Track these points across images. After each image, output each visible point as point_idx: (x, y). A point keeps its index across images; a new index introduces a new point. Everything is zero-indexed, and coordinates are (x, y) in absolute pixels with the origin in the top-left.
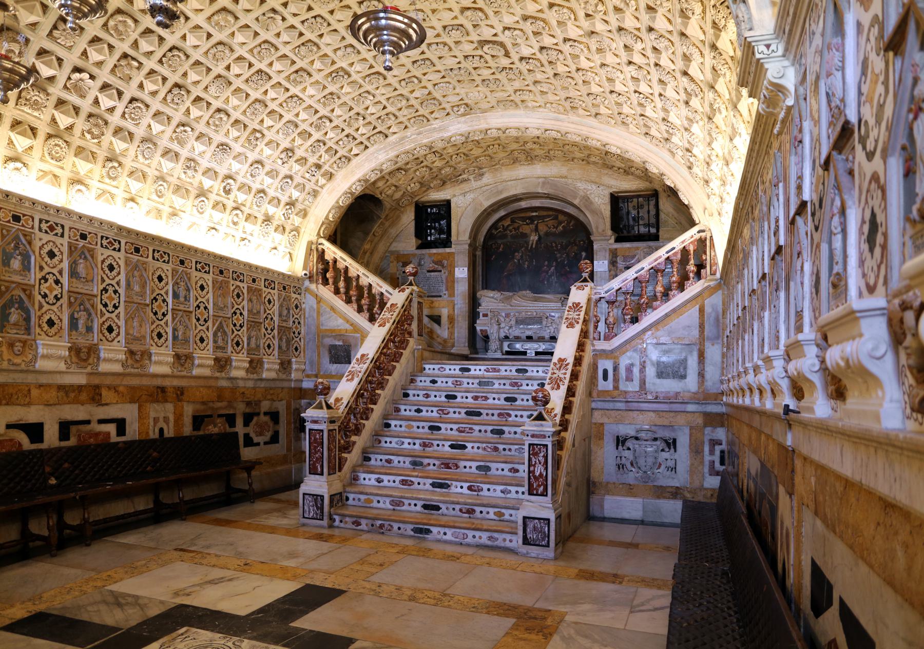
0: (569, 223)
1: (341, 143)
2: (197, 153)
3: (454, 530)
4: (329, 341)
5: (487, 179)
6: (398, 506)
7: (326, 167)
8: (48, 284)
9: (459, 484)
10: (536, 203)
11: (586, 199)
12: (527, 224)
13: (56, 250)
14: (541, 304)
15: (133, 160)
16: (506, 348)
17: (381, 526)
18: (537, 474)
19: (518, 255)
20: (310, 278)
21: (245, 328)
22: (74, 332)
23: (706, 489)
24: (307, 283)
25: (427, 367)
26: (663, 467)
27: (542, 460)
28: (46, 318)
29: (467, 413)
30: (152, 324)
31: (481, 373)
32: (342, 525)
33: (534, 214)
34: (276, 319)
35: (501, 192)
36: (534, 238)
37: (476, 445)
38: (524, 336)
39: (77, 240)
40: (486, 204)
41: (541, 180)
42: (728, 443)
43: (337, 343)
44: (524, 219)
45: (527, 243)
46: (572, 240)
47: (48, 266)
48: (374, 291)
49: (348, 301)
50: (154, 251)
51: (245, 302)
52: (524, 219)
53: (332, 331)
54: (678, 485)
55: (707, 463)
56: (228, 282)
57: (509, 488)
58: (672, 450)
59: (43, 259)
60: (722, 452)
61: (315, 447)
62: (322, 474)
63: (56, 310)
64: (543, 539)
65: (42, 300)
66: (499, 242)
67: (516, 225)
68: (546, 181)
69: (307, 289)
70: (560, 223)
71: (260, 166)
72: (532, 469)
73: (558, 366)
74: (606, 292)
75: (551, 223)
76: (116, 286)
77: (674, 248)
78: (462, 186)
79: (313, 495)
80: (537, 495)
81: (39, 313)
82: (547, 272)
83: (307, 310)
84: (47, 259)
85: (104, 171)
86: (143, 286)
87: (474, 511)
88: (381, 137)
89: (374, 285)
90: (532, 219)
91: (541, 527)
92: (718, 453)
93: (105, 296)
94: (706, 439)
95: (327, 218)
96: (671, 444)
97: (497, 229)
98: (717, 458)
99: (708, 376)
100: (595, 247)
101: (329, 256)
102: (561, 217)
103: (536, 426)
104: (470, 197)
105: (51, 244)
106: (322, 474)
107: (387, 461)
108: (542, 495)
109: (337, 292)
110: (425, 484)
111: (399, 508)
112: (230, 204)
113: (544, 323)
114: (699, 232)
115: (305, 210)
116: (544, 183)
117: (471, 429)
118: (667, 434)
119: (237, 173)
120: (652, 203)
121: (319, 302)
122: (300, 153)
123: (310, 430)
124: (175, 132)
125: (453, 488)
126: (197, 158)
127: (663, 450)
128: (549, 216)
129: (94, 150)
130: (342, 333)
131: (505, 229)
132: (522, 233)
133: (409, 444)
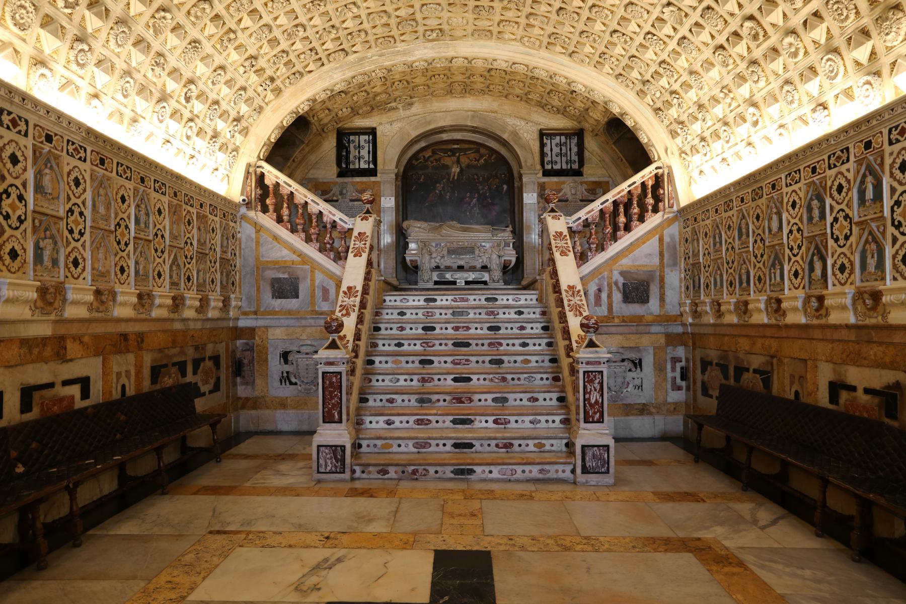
0: (490, 157)
1: (302, 56)
2: (168, 47)
3: (501, 467)
4: (271, 274)
5: (417, 109)
6: (424, 447)
7: (278, 82)
9: (483, 418)
10: (458, 136)
11: (515, 134)
14: (471, 234)
15: (103, 46)
16: (435, 278)
17: (414, 472)
18: (593, 401)
19: (439, 186)
20: (248, 204)
21: (194, 261)
22: (39, 267)
23: (669, 403)
24: (243, 210)
25: (387, 298)
26: (631, 386)
27: (598, 387)
29: (454, 345)
30: (116, 255)
31: (448, 303)
32: (364, 476)
33: (456, 146)
34: (218, 249)
35: (429, 123)
36: (455, 170)
37: (482, 377)
38: (455, 266)
40: (414, 134)
41: (469, 113)
42: (687, 360)
43: (281, 276)
45: (449, 175)
46: (494, 173)
47: (11, 175)
48: (325, 219)
49: (293, 231)
51: (195, 231)
52: (445, 151)
53: (275, 262)
54: (644, 402)
55: (669, 380)
56: (181, 206)
57: (538, 417)
58: (639, 369)
59: (4, 165)
60: (682, 368)
61: (331, 392)
62: (340, 421)
63: (19, 236)
64: (603, 466)
66: (420, 172)
67: (437, 157)
68: (475, 114)
69: (244, 217)
70: (482, 156)
71: (223, 73)
72: (587, 396)
73: (570, 293)
74: (574, 222)
75: (472, 156)
76: (81, 205)
77: (635, 183)
78: (390, 114)
79: (331, 446)
80: (593, 422)
82: (470, 204)
83: (243, 240)
85: (72, 54)
86: (108, 208)
87: (512, 445)
88: (342, 54)
89: (325, 212)
90: (453, 151)
91: (601, 454)
92: (678, 370)
94: (669, 357)
95: (269, 139)
96: (638, 364)
97: (417, 160)
98: (678, 374)
99: (668, 299)
100: (524, 180)
101: (269, 181)
102: (482, 151)
103: (591, 353)
104: (396, 126)
105: (14, 144)
106: (340, 421)
107: (388, 401)
108: (598, 422)
109: (279, 220)
110: (444, 422)
111: (424, 450)
112: (187, 115)
113: (477, 252)
114: (657, 168)
115: (247, 128)
116: (473, 117)
117: (467, 360)
118: (633, 355)
119: (199, 78)
120: (575, 141)
121: (258, 231)
122: (261, 63)
123: (323, 373)
124: (153, 17)
125: (476, 423)
126: (167, 53)
127: (630, 370)
128: (470, 149)
129: (64, 24)
130: (288, 264)
132: (443, 165)
133: (406, 380)
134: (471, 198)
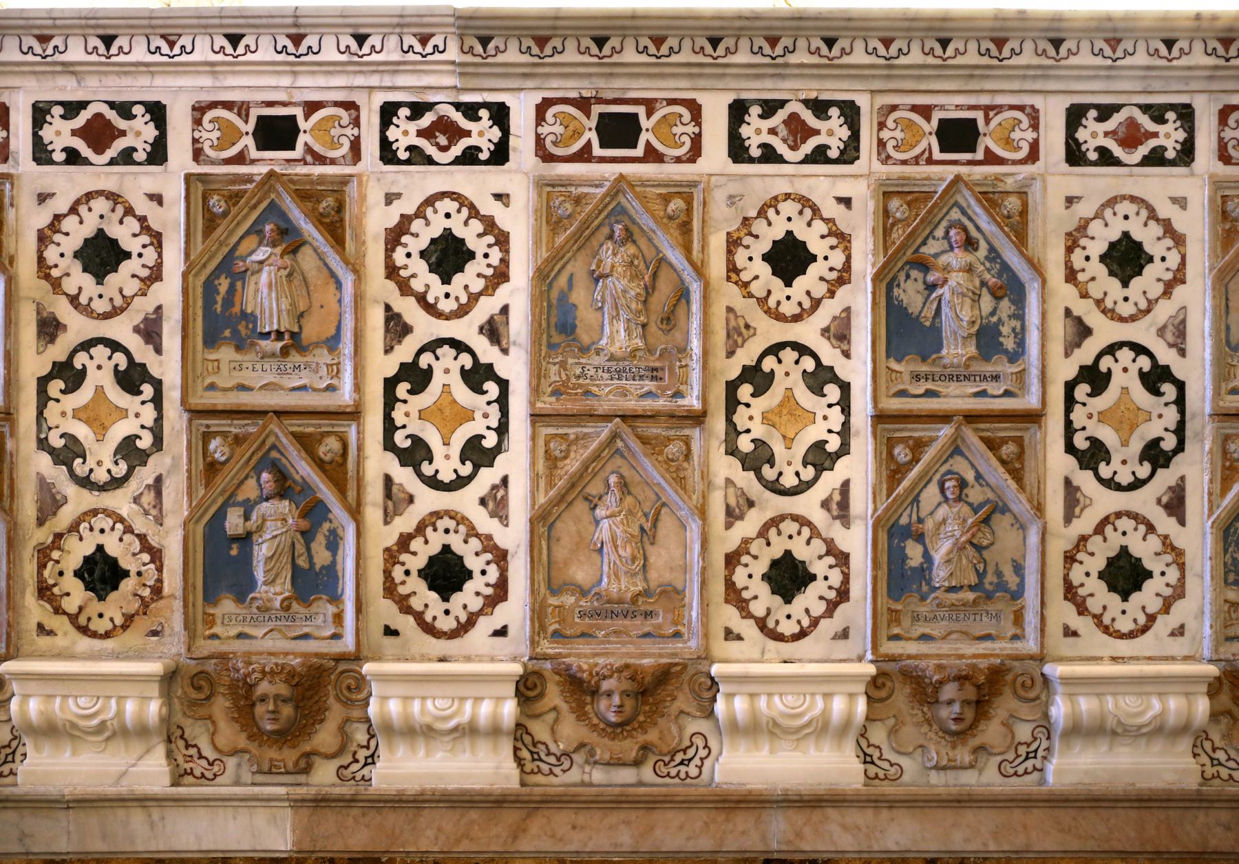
8: (84, 394)
13: (125, 234)
22: (228, 605)
28: (78, 551)
30: (733, 516)
39: (240, 159)
47: (87, 311)
50: (738, 111)
59: (56, 285)
65: (57, 475)
81: (43, 536)
84: (79, 280)
93: (410, 412)
105: (100, 205)
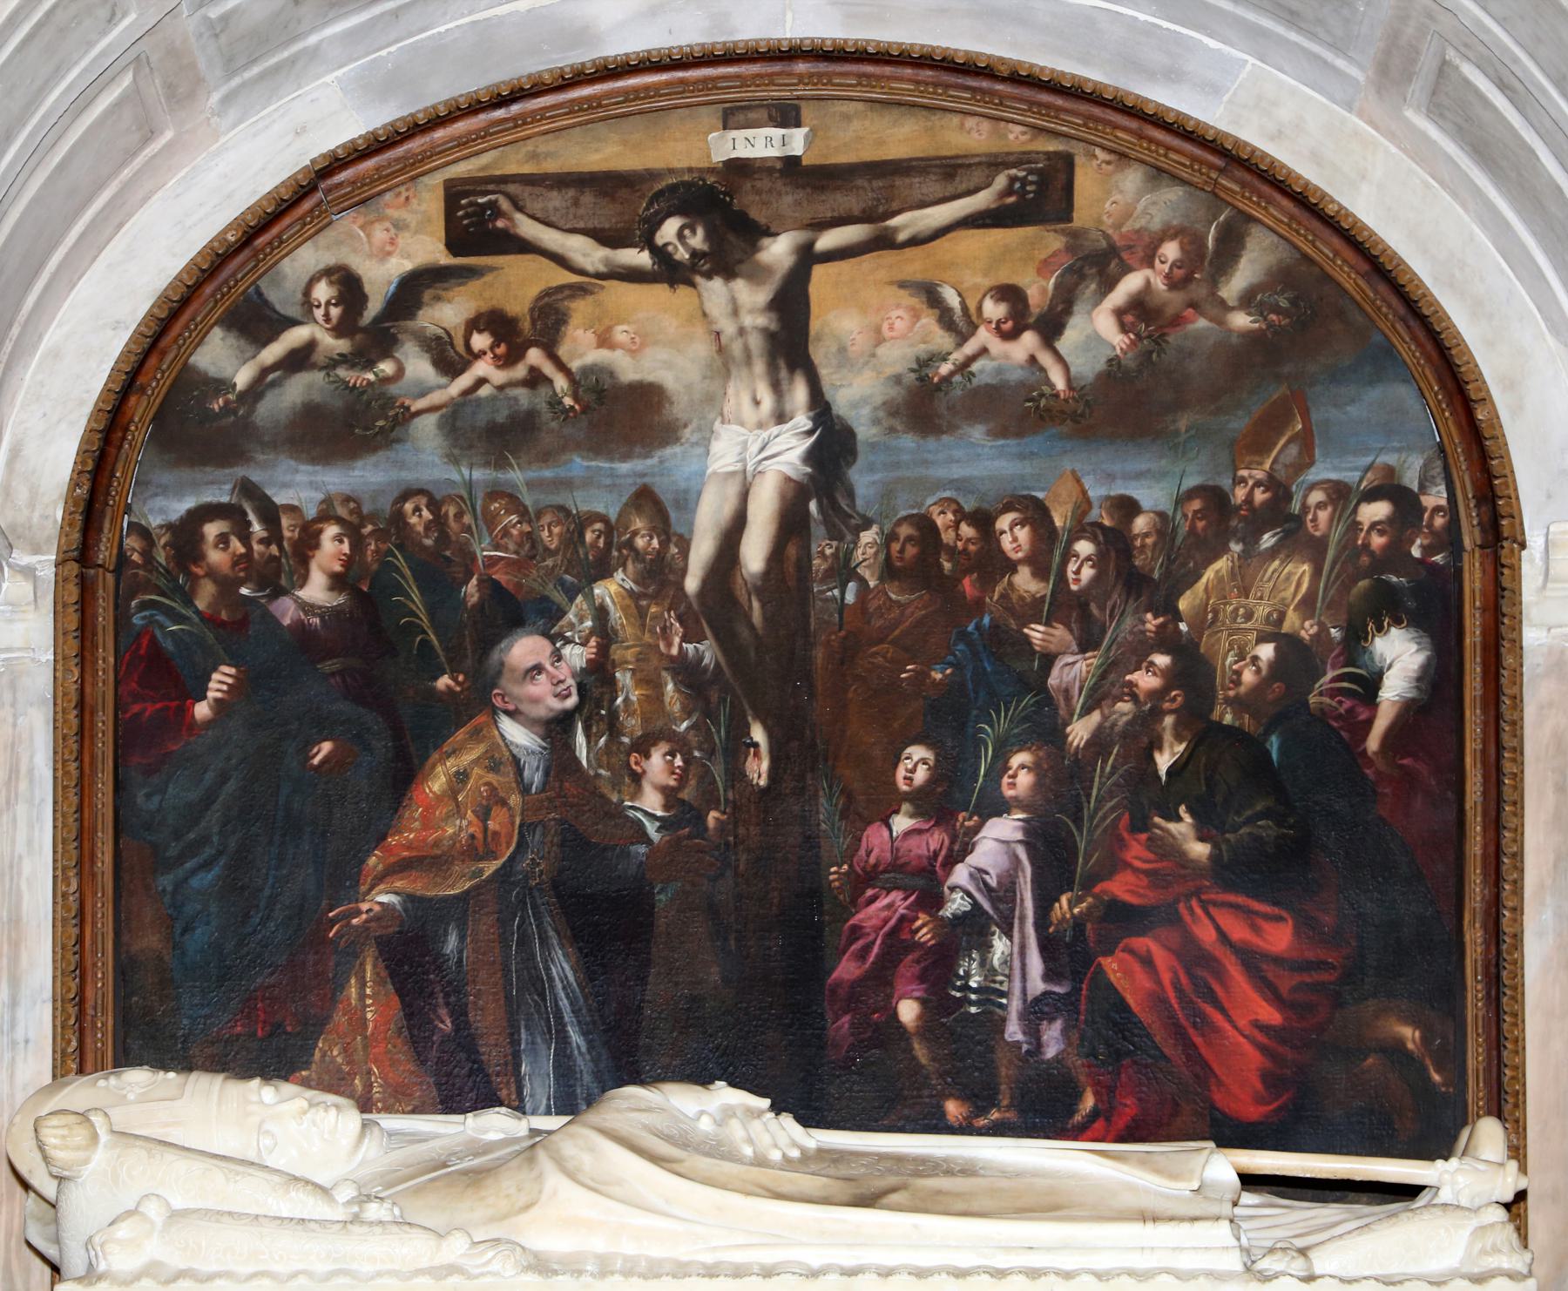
12: (670, 272)
33: (761, 143)
44: (622, 205)
46: (1248, 489)
52: (622, 205)
67: (516, 284)
70: (1097, 264)
75: (977, 263)
90: (725, 213)
102: (1111, 194)
128: (950, 172)
131: (373, 326)
134: (954, 802)
